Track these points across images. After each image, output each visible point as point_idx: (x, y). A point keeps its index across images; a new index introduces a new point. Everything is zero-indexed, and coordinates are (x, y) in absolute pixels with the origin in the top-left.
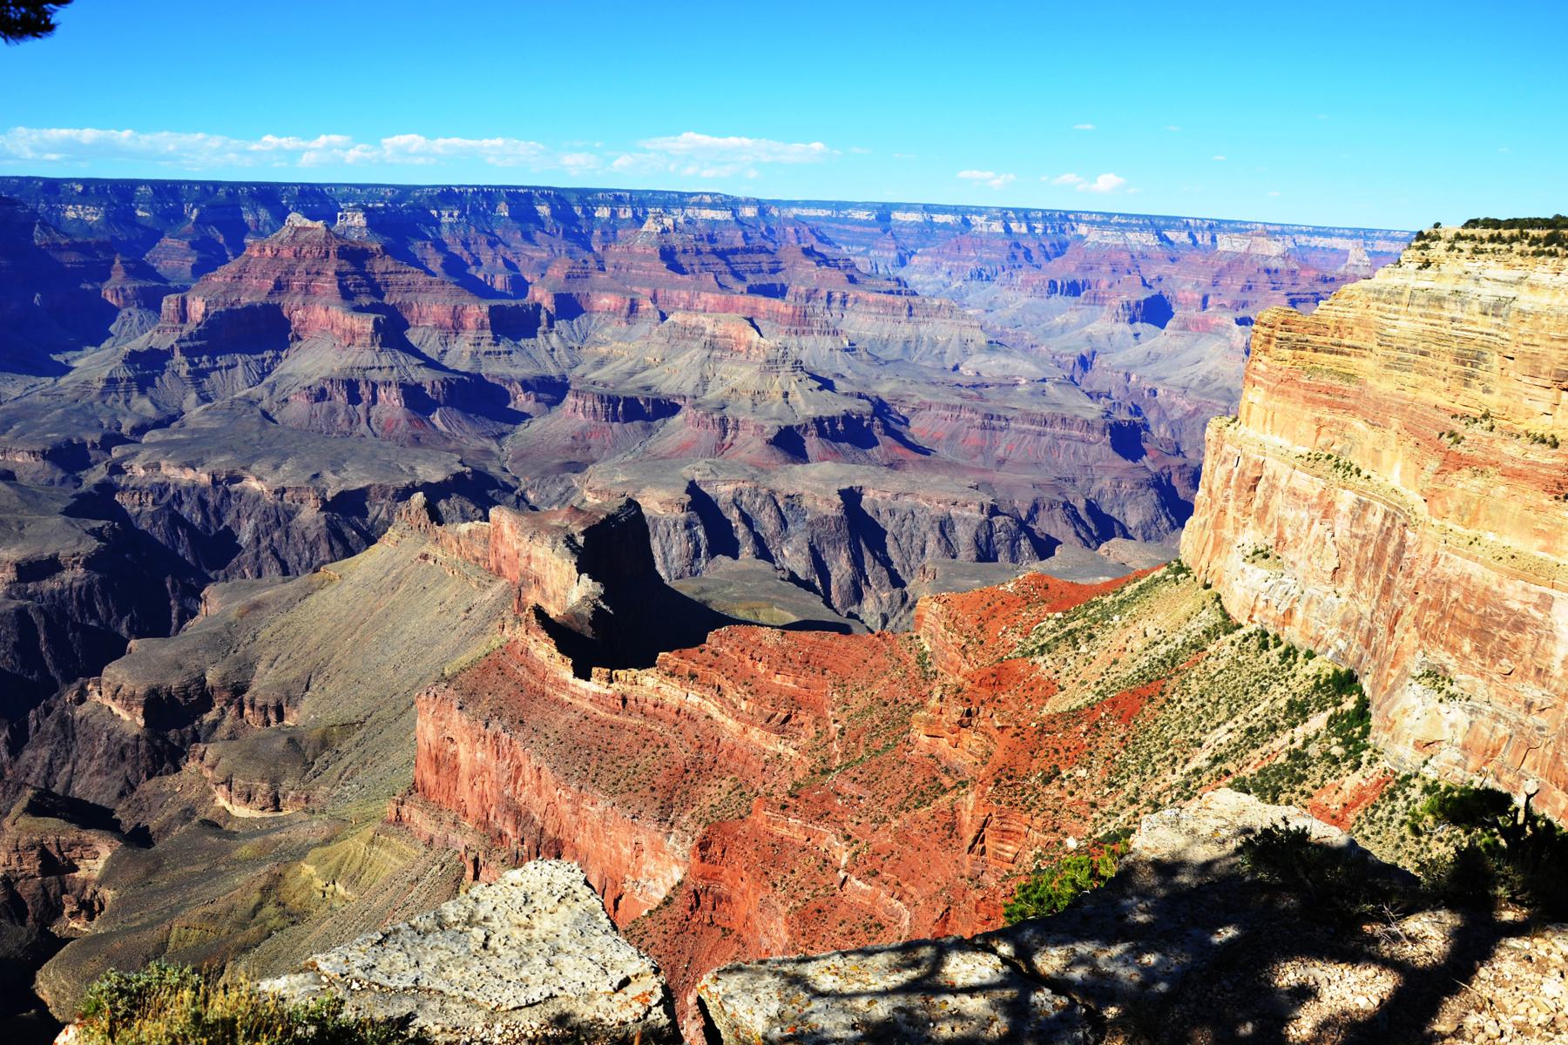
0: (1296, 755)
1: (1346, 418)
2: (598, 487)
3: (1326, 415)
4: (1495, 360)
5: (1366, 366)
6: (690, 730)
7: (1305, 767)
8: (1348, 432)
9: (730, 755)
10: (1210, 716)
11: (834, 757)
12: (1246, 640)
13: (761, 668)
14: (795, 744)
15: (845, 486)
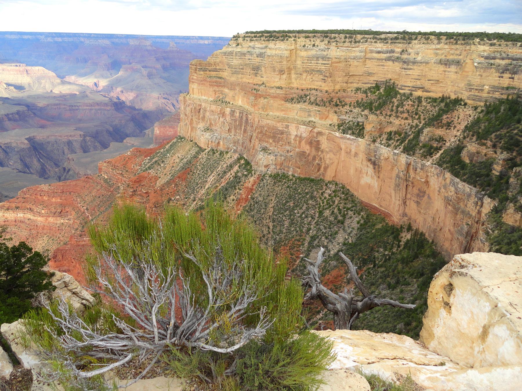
0: (236, 177)
1: (222, 89)
3: (216, 88)
4: (263, 69)
5: (225, 74)
6: (23, 225)
7: (239, 179)
8: (223, 93)
9: (43, 229)
10: (207, 174)
11: (88, 217)
13: (45, 198)
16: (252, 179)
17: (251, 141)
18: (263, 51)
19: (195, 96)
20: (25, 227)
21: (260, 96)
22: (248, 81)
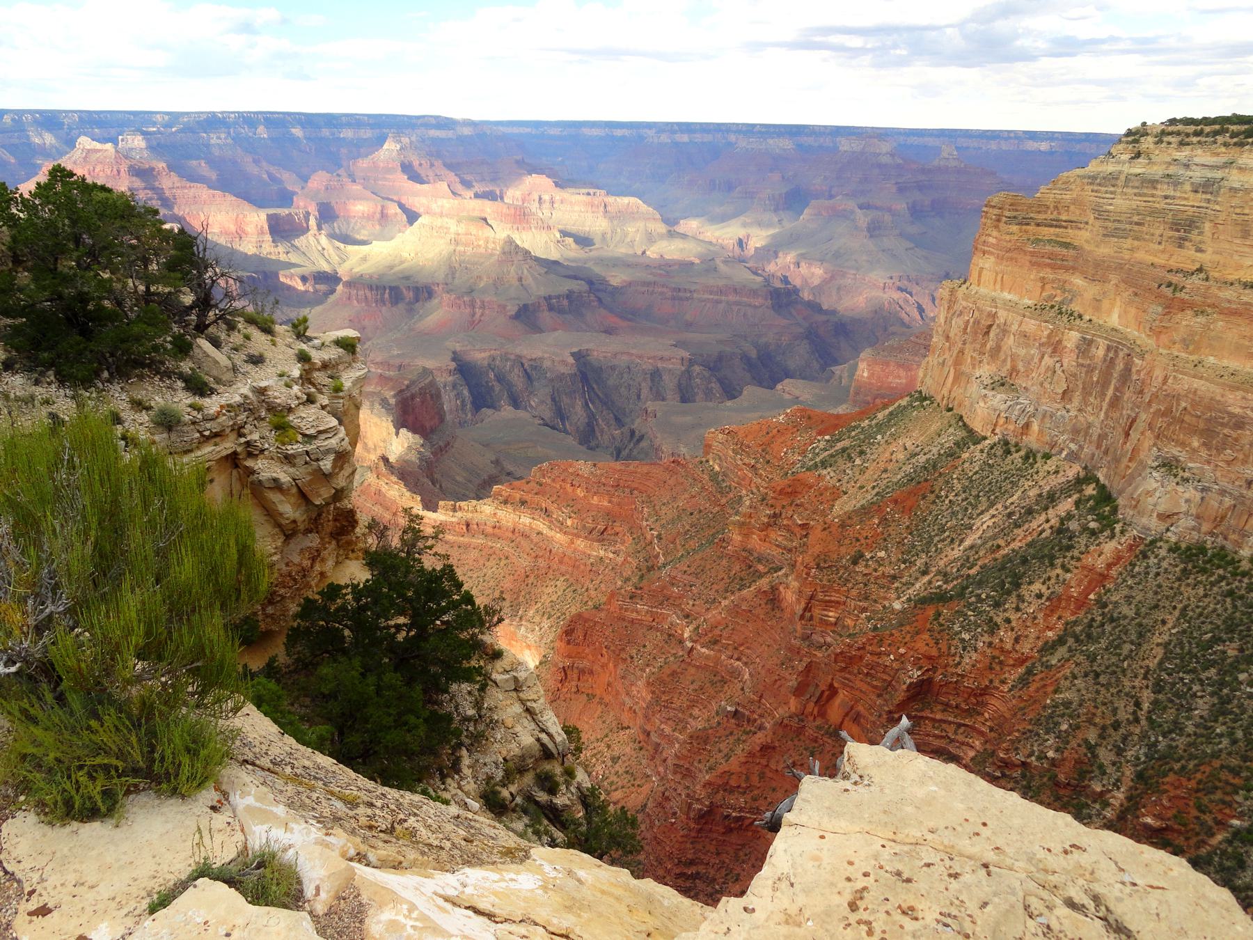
0: (1060, 531)
1: (1066, 276)
2: (378, 360)
3: (1048, 274)
4: (1207, 226)
5: (1081, 237)
6: (525, 544)
7: (1070, 538)
8: (1067, 287)
9: (561, 562)
10: (975, 507)
11: (657, 556)
12: (992, 448)
13: (580, 493)
14: (612, 549)
15: (575, 350)
16: (1109, 547)
17: (1127, 435)
18: (1219, 174)
19: (983, 290)
20: (528, 550)
21: (1184, 306)
22: (1150, 259)
